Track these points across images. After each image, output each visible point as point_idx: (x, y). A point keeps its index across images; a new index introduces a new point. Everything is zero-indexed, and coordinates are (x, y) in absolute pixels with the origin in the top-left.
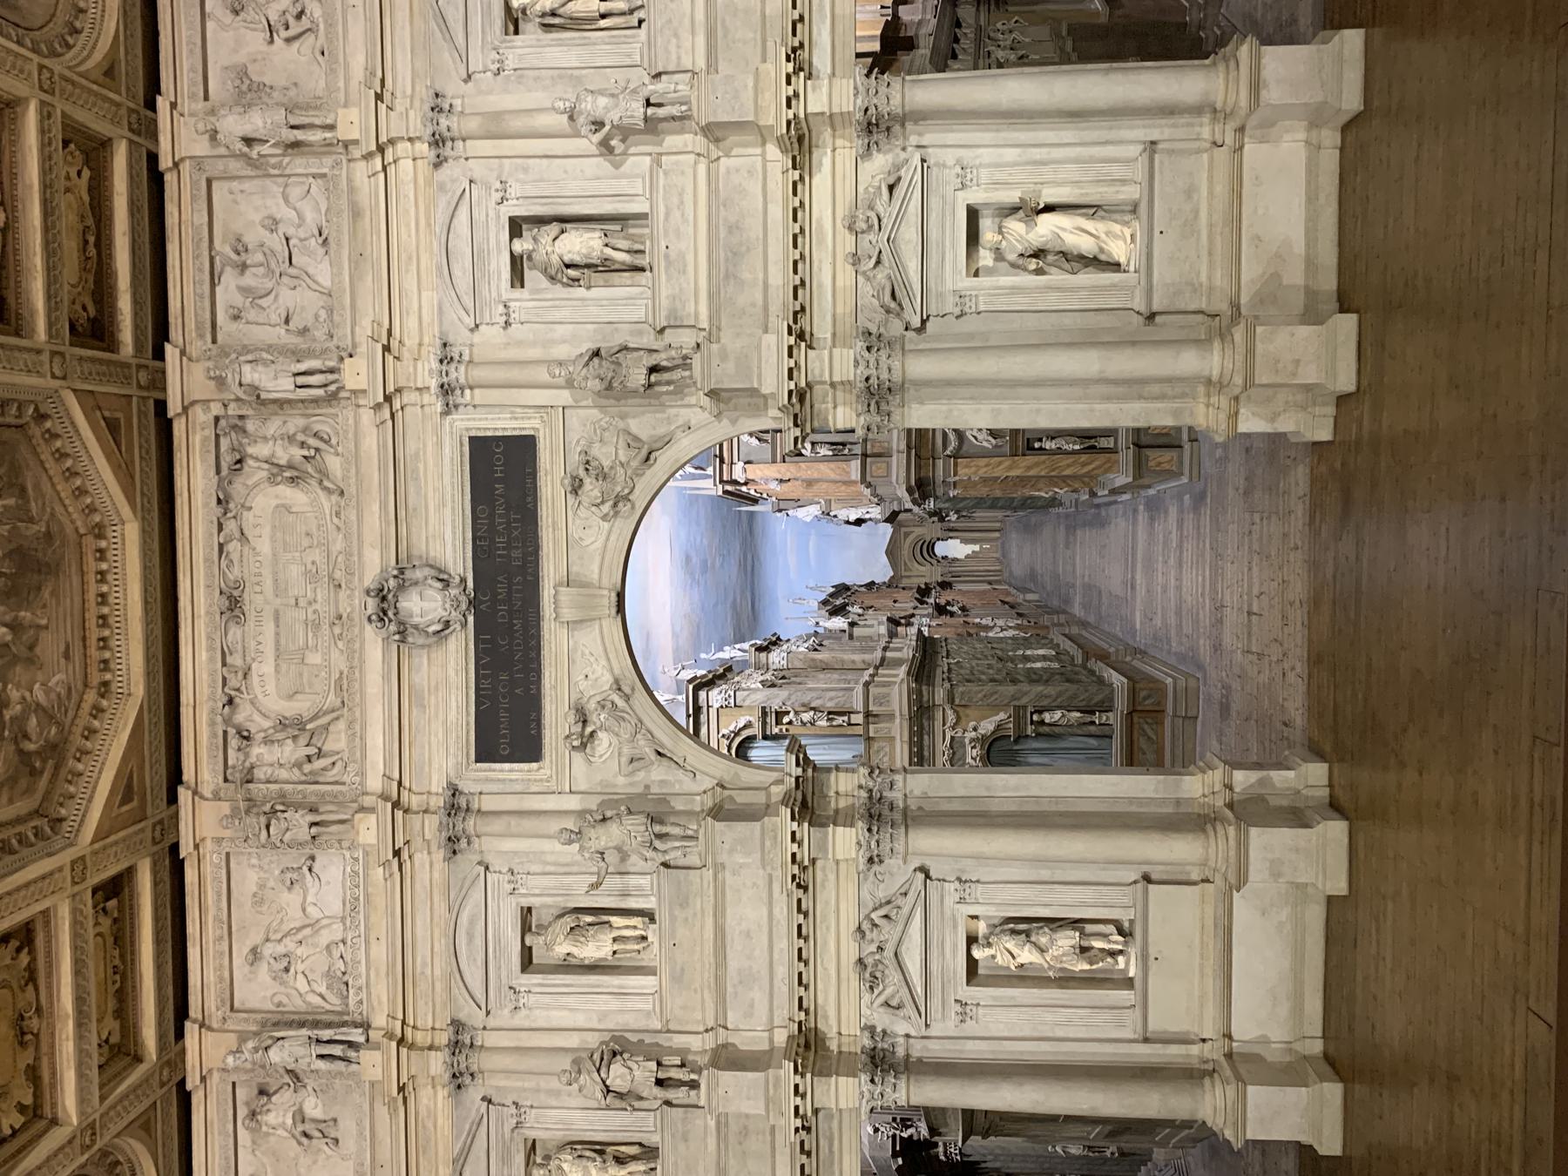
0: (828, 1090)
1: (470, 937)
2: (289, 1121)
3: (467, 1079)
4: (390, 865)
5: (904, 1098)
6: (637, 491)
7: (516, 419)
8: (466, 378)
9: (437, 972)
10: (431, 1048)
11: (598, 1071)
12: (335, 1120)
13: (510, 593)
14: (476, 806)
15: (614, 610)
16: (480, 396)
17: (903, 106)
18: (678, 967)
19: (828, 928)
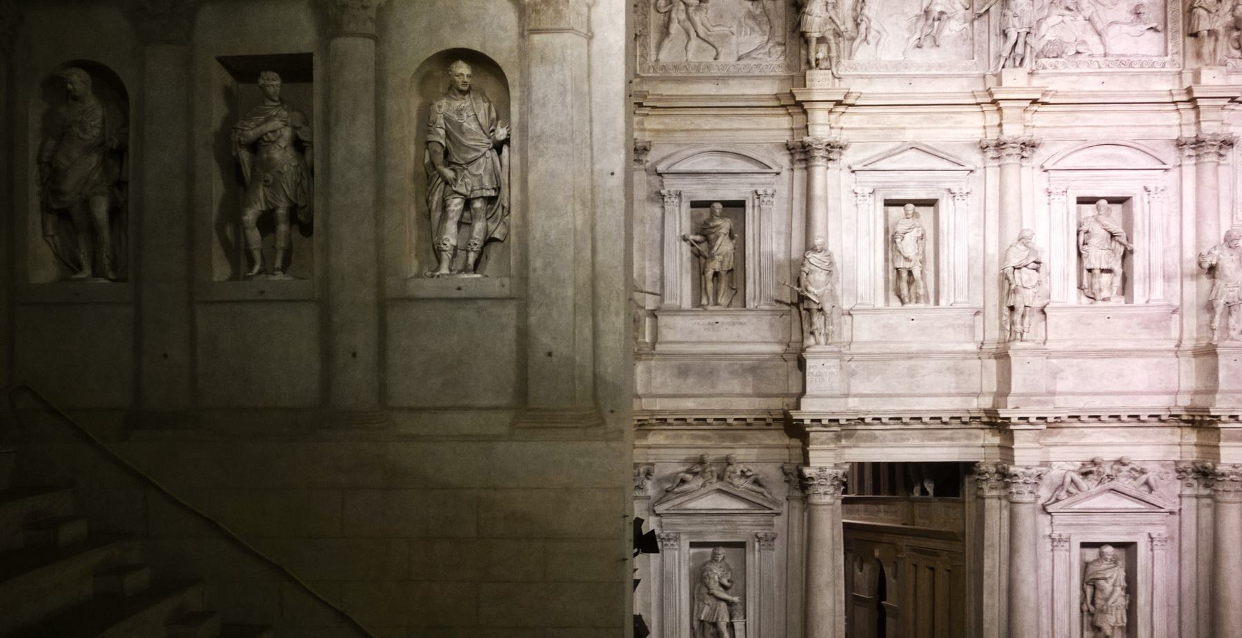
1: (1106, 157)
2: (939, 9)
3: (991, 153)
4: (1180, 94)
9: (1078, 131)
10: (1025, 126)
11: (1035, 262)
12: (938, 46)
14: (1221, 162)
18: (1090, 321)
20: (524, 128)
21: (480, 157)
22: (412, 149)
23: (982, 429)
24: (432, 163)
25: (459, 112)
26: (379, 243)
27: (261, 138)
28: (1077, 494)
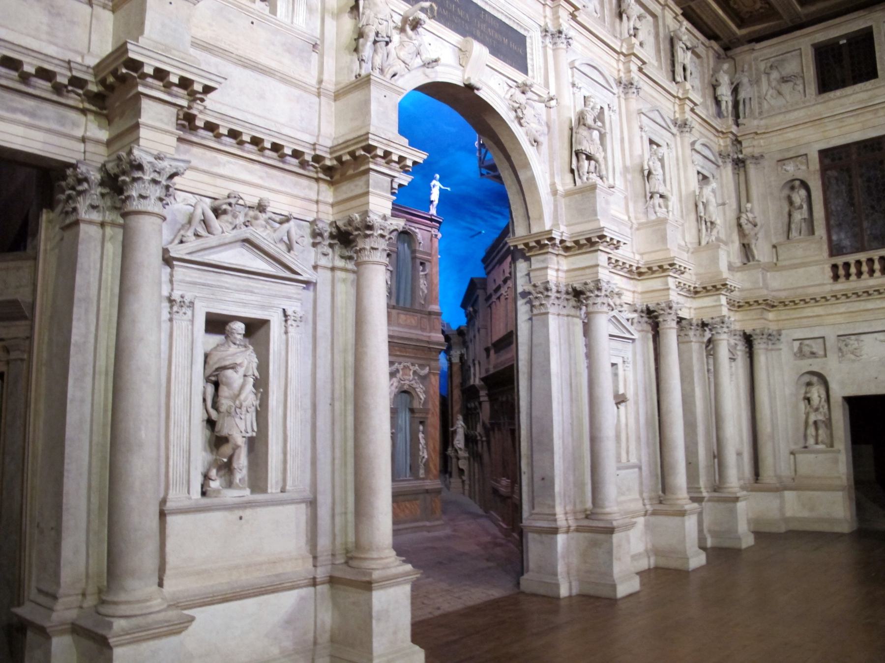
0: (161, 121)
5: (150, 209)
6: (518, 126)
7: (540, 68)
8: (562, 48)
13: (459, 16)
15: (474, 82)
16: (550, 52)
17: (670, 328)
19: (261, 178)
23: (84, 111)
28: (207, 237)
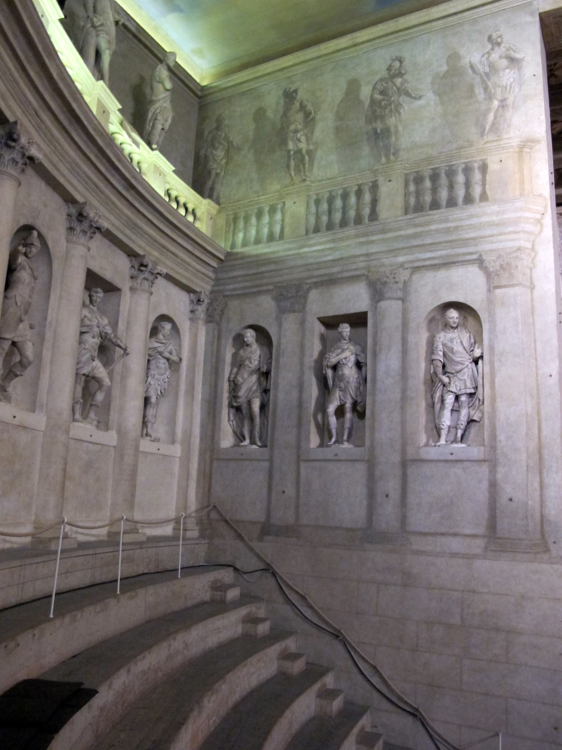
20: (492, 348)
21: (465, 368)
22: (423, 365)
24: (435, 373)
25: (451, 340)
26: (403, 423)
27: (339, 362)
